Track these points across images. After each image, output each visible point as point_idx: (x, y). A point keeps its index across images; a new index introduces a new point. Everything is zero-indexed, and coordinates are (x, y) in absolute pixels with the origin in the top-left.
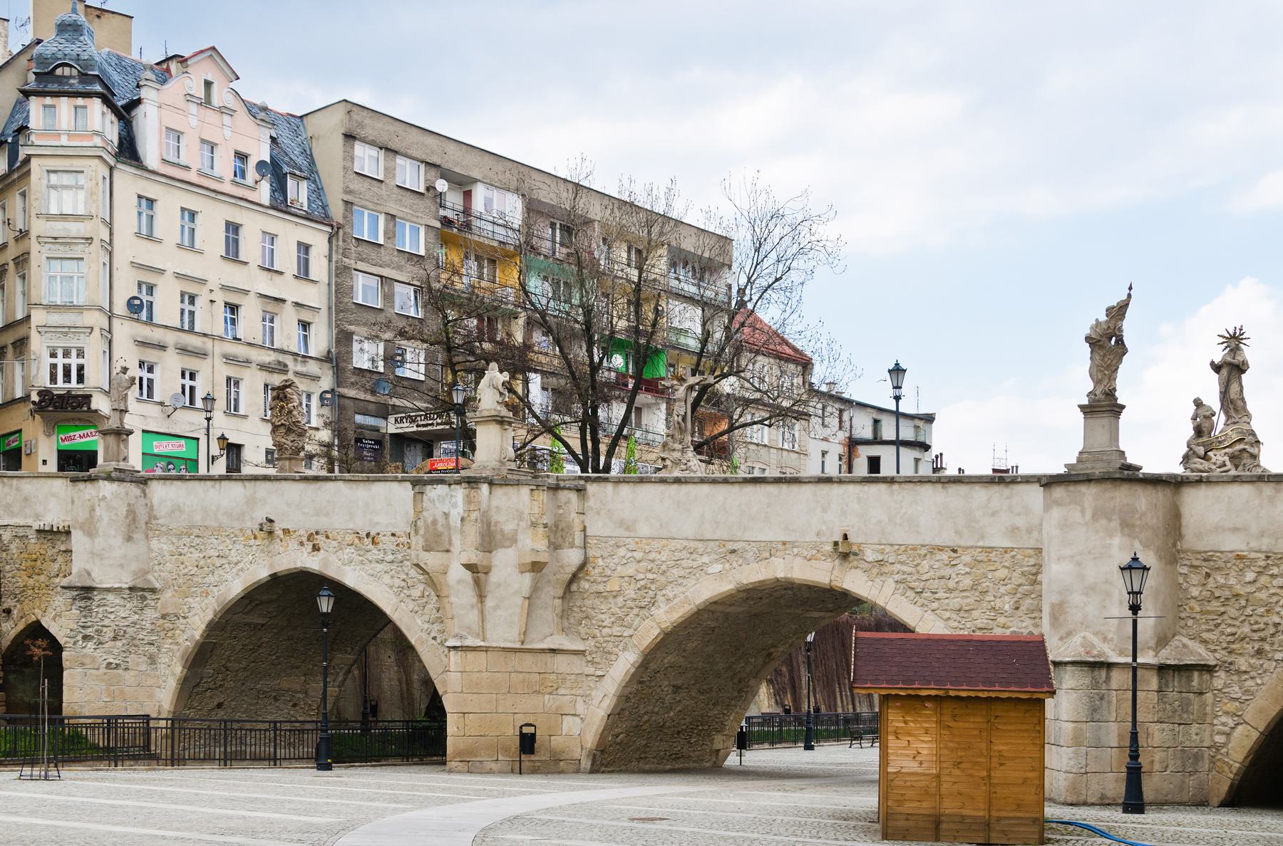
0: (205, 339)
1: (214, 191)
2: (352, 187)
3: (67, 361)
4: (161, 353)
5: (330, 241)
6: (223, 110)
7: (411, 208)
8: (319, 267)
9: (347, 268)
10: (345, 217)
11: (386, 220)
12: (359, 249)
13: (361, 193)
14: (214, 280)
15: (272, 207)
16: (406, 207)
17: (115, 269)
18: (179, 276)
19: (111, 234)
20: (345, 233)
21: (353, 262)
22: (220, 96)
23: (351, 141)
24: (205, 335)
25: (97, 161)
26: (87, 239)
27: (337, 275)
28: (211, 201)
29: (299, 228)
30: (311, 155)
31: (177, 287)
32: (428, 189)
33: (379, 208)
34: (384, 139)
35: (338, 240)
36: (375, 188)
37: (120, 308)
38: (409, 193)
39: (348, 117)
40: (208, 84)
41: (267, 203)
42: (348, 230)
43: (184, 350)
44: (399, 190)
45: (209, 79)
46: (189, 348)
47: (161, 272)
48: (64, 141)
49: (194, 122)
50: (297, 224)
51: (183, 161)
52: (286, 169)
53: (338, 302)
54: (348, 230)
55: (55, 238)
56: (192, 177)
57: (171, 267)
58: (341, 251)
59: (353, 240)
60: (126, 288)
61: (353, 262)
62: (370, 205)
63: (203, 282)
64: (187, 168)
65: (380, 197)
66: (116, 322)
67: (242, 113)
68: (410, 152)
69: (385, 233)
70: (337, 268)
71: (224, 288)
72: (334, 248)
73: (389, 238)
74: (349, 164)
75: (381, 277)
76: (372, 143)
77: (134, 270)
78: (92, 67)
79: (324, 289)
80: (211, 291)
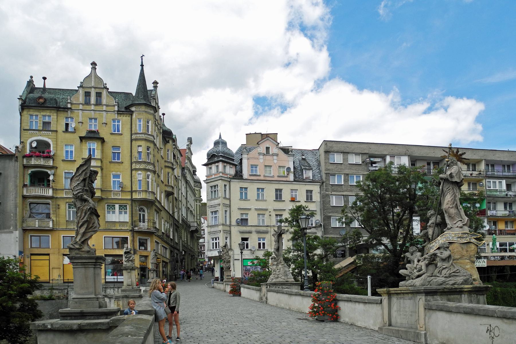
0: (267, 227)
1: (269, 181)
2: (329, 168)
3: (216, 241)
4: (250, 234)
5: (320, 188)
6: (273, 155)
7: (356, 170)
8: (316, 197)
9: (328, 196)
10: (326, 178)
11: (344, 176)
12: (333, 188)
13: (333, 169)
14: (271, 208)
15: (295, 181)
16: (353, 170)
17: (231, 211)
18: (256, 209)
19: (230, 201)
20: (326, 184)
21: (330, 192)
22: (274, 150)
23: (328, 153)
24: (267, 226)
25: (221, 181)
26: (219, 204)
27: (323, 198)
28: (269, 184)
29: (306, 185)
30: (320, 161)
31: (256, 213)
32: (363, 162)
33: (341, 173)
34: (343, 149)
35: (323, 187)
36: (339, 167)
37: (234, 222)
38: (354, 165)
39: (326, 146)
40: (268, 148)
41: (293, 180)
42: (327, 182)
43: (258, 232)
44: (350, 165)
45: (268, 146)
46: (261, 231)
47: (250, 209)
48: (213, 177)
49: (261, 161)
50: (305, 184)
51: (258, 174)
52: (303, 167)
53: (324, 207)
54: (327, 182)
55: (211, 206)
56: (262, 178)
57: (253, 207)
58: (325, 190)
59: (330, 185)
60: (236, 216)
61: (330, 192)
62: (337, 172)
63: (266, 210)
64: (260, 176)
65: (342, 169)
66: (232, 228)
67: (281, 153)
68: (354, 152)
69: (344, 181)
70: (323, 196)
71: (274, 210)
72: (322, 189)
73: (346, 182)
74: (327, 161)
75: (343, 195)
76: (337, 152)
77: (239, 211)
78: (219, 153)
79: (319, 204)
80: (270, 212)
